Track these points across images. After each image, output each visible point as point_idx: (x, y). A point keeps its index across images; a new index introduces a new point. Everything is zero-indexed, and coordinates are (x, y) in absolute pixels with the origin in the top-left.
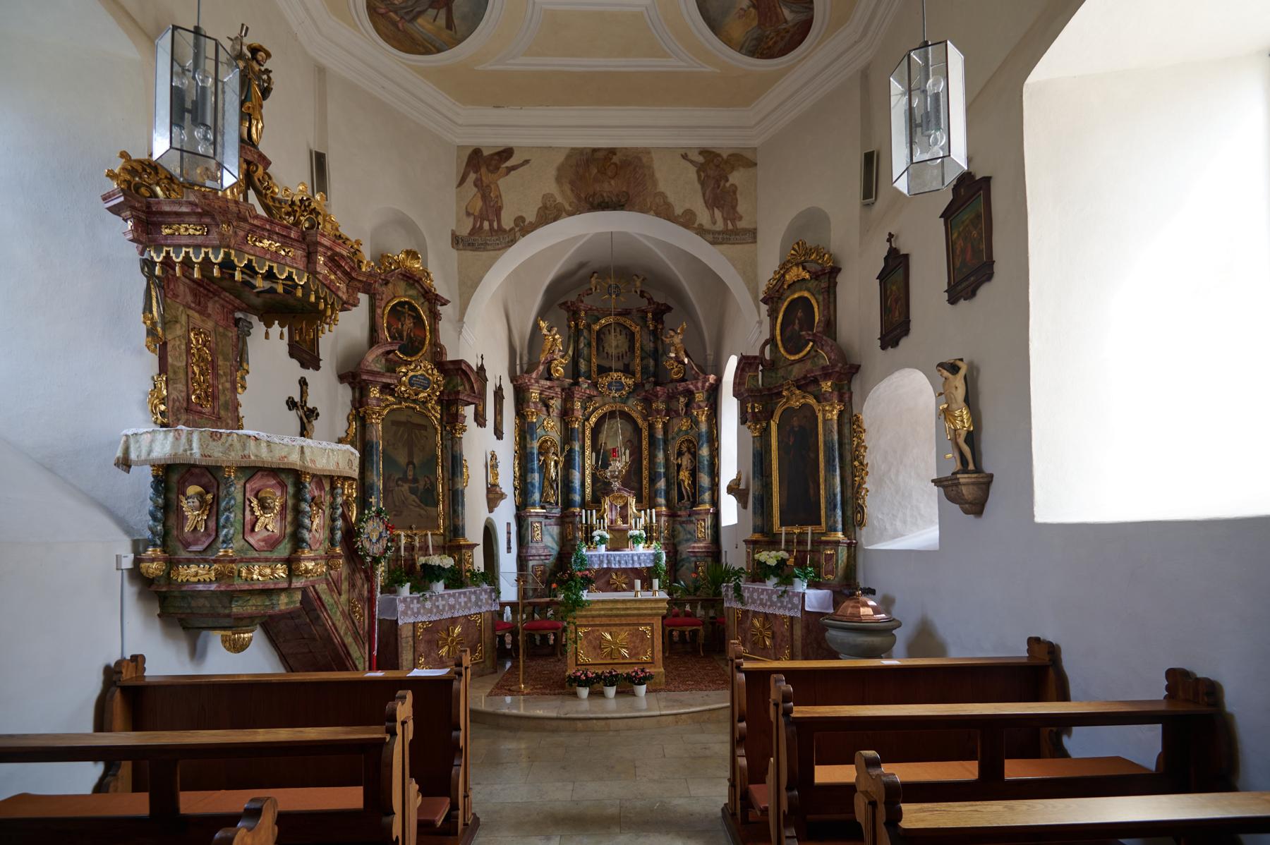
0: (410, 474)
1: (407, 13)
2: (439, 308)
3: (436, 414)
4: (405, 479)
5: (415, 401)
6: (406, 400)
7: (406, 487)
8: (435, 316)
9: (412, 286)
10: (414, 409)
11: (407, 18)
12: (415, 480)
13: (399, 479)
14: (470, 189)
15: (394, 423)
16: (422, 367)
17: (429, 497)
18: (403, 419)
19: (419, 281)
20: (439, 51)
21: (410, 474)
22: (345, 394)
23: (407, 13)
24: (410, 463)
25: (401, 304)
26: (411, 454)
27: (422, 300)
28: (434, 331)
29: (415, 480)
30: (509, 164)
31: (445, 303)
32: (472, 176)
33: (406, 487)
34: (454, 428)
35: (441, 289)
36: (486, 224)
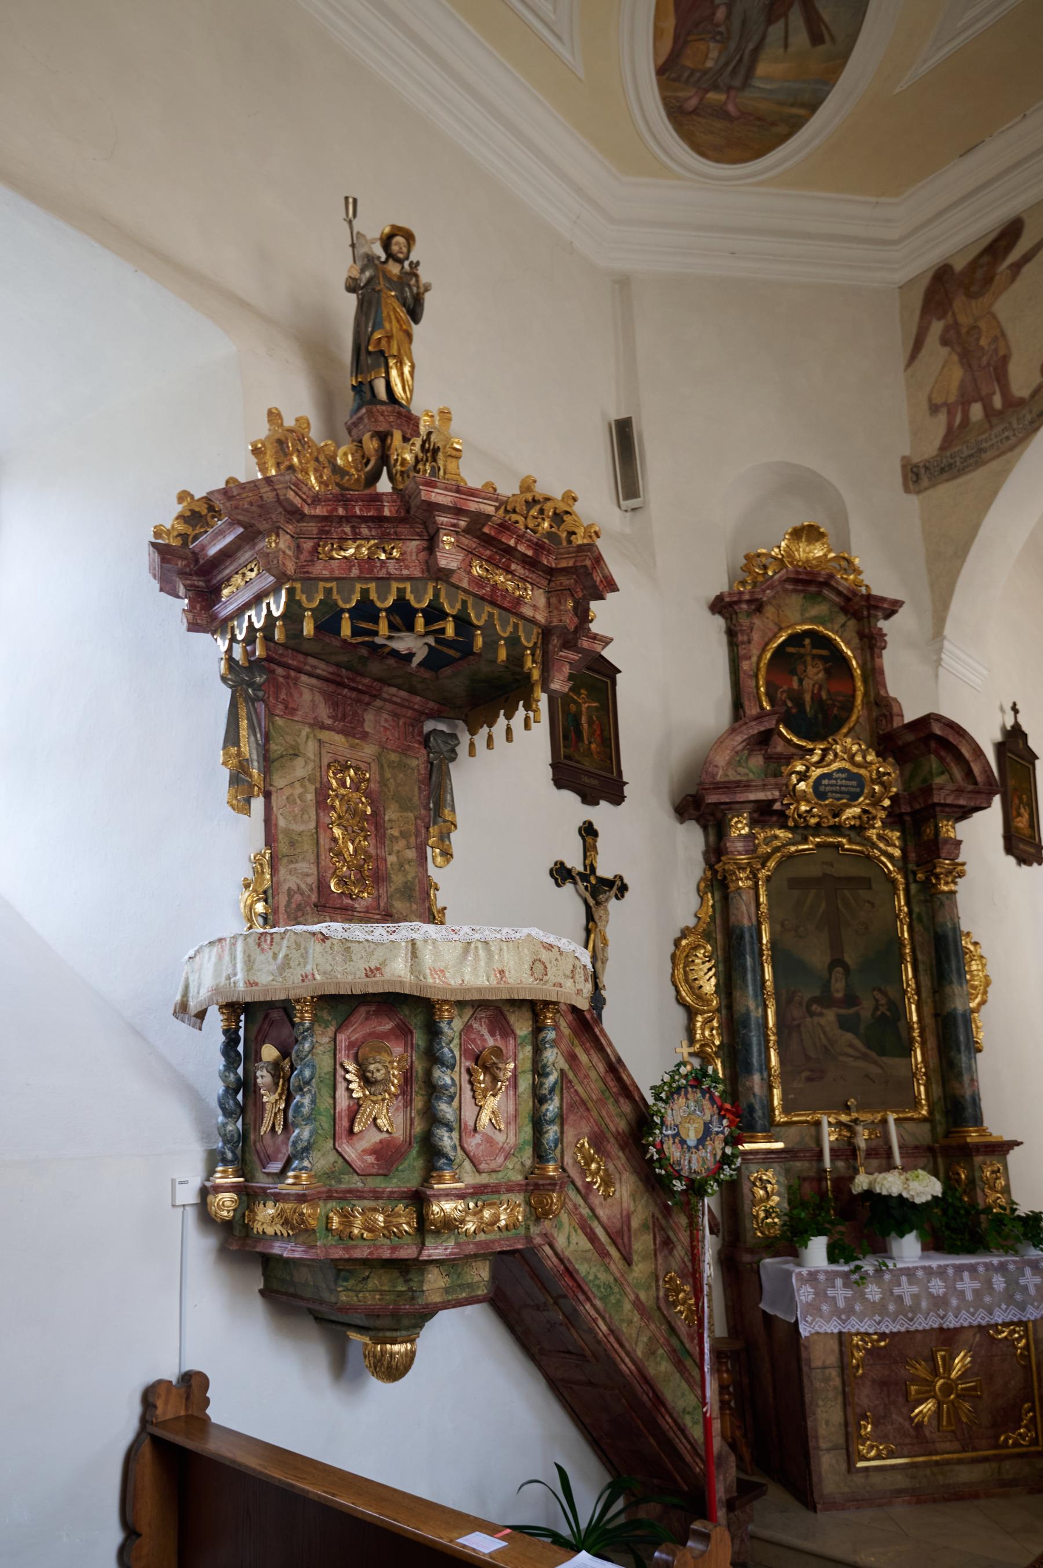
0: (838, 988)
1: (734, 72)
2: (882, 624)
3: (889, 847)
4: (826, 1000)
5: (837, 829)
6: (817, 829)
7: (830, 1016)
8: (872, 643)
9: (816, 598)
10: (840, 845)
11: (737, 82)
12: (851, 1000)
13: (815, 1000)
14: (936, 354)
15: (795, 883)
16: (849, 751)
17: (887, 1035)
18: (814, 871)
19: (828, 583)
20: (813, 107)
21: (838, 988)
22: (690, 840)
23: (734, 72)
24: (837, 962)
25: (795, 639)
26: (836, 945)
27: (842, 618)
28: (874, 675)
29: (851, 1000)
30: (1014, 256)
31: (891, 608)
32: (937, 327)
33: (830, 1016)
34: (931, 873)
35: (878, 579)
36: (976, 411)
